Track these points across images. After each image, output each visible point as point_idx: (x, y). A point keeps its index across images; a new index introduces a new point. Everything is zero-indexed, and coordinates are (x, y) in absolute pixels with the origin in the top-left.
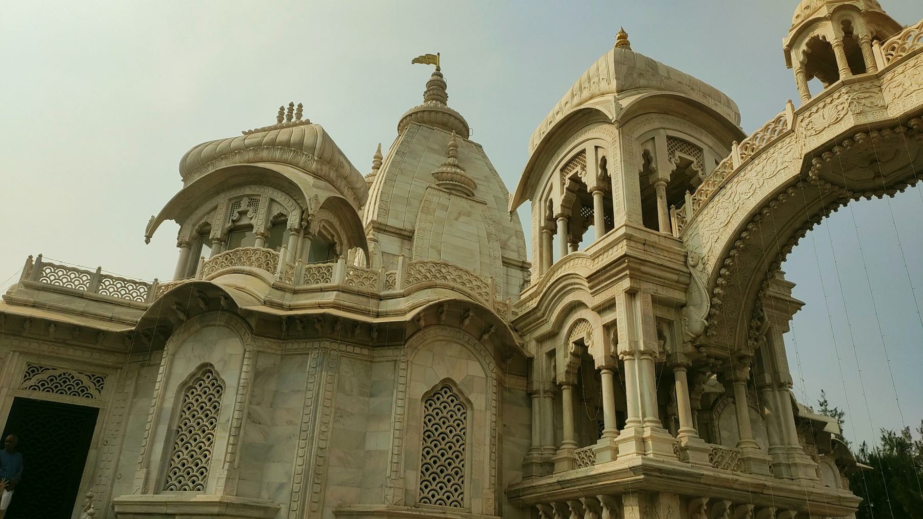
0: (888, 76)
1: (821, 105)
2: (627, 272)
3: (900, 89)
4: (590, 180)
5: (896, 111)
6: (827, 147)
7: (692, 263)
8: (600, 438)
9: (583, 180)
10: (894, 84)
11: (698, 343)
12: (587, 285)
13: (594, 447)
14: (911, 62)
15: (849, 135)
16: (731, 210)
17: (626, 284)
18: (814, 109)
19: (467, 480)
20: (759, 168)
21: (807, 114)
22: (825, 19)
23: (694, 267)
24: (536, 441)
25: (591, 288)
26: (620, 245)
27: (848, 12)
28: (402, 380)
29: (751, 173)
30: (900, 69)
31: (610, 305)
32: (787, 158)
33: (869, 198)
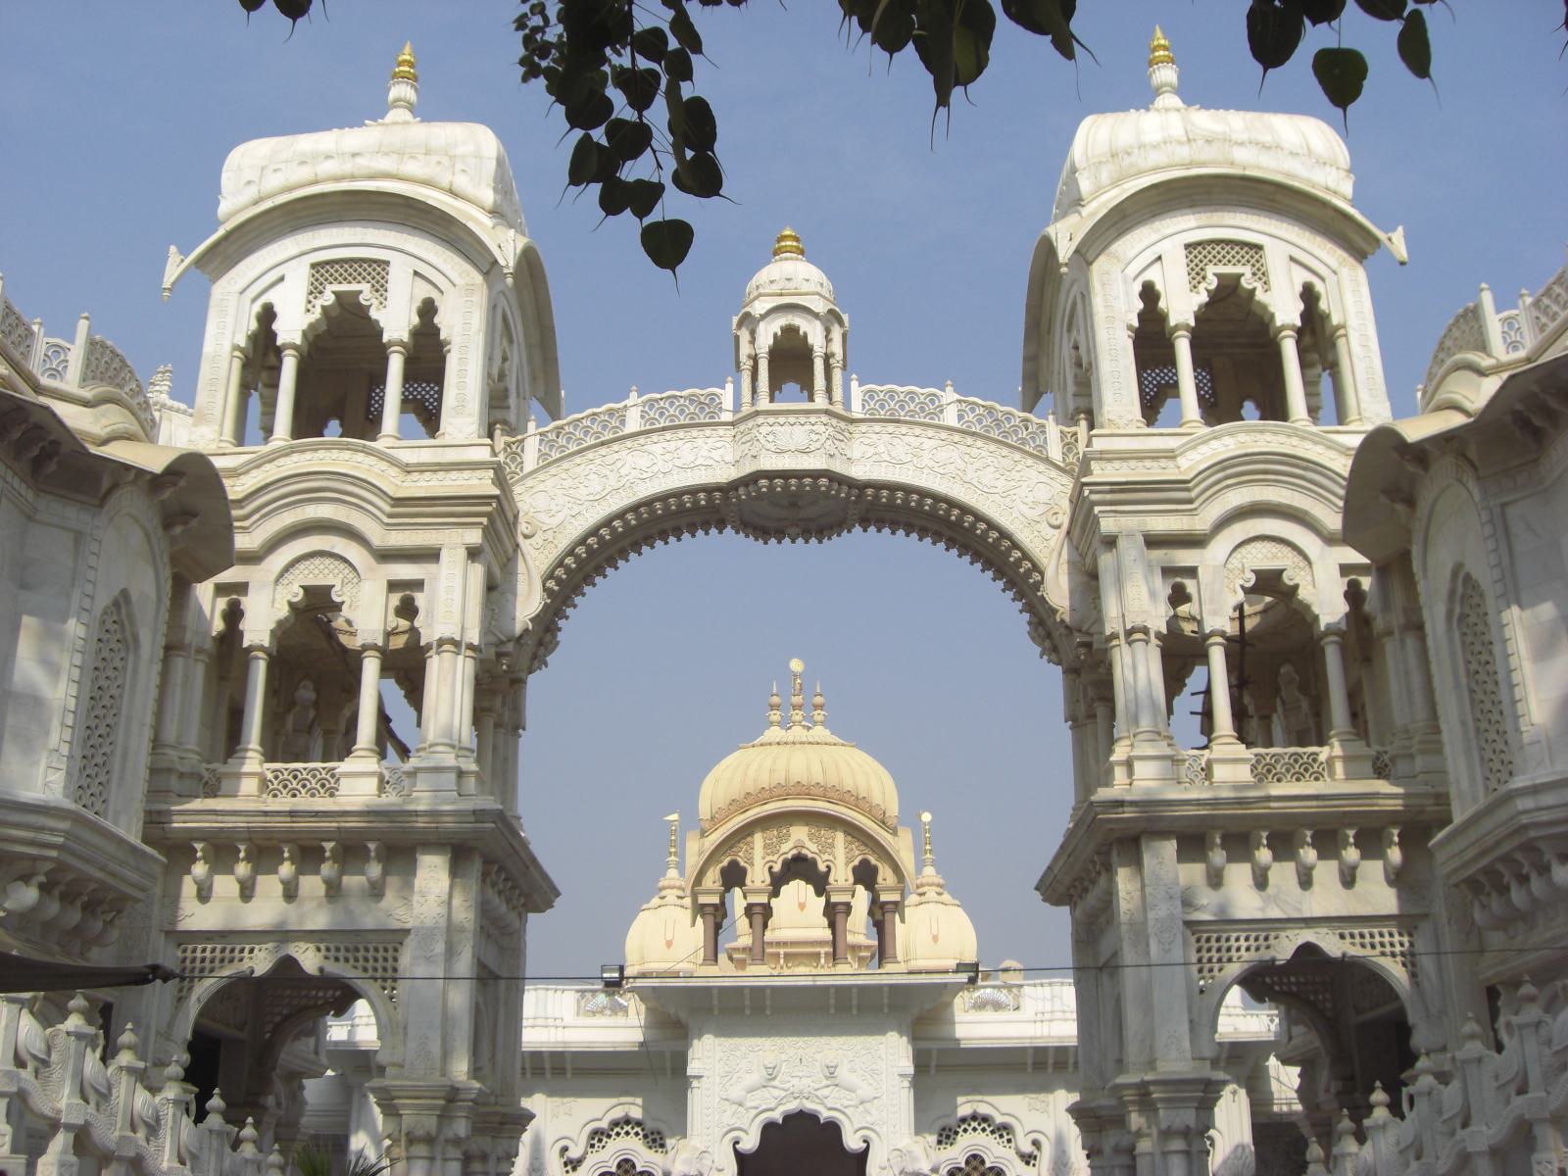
0: (864, 427)
1: (792, 419)
2: (484, 520)
3: (871, 450)
4: (395, 321)
5: (860, 472)
6: (785, 475)
7: (526, 532)
8: (347, 756)
9: (374, 314)
10: (867, 441)
11: (504, 649)
12: (387, 509)
13: (343, 767)
14: (891, 427)
15: (816, 475)
16: (612, 482)
17: (475, 537)
18: (782, 420)
19: (115, 776)
20: (673, 445)
21: (771, 420)
22: (816, 316)
23: (526, 537)
24: (170, 733)
25: (390, 516)
26: (478, 473)
27: (833, 320)
28: (91, 575)
29: (657, 446)
30: (877, 427)
31: (431, 555)
32: (716, 455)
33: (747, 536)
